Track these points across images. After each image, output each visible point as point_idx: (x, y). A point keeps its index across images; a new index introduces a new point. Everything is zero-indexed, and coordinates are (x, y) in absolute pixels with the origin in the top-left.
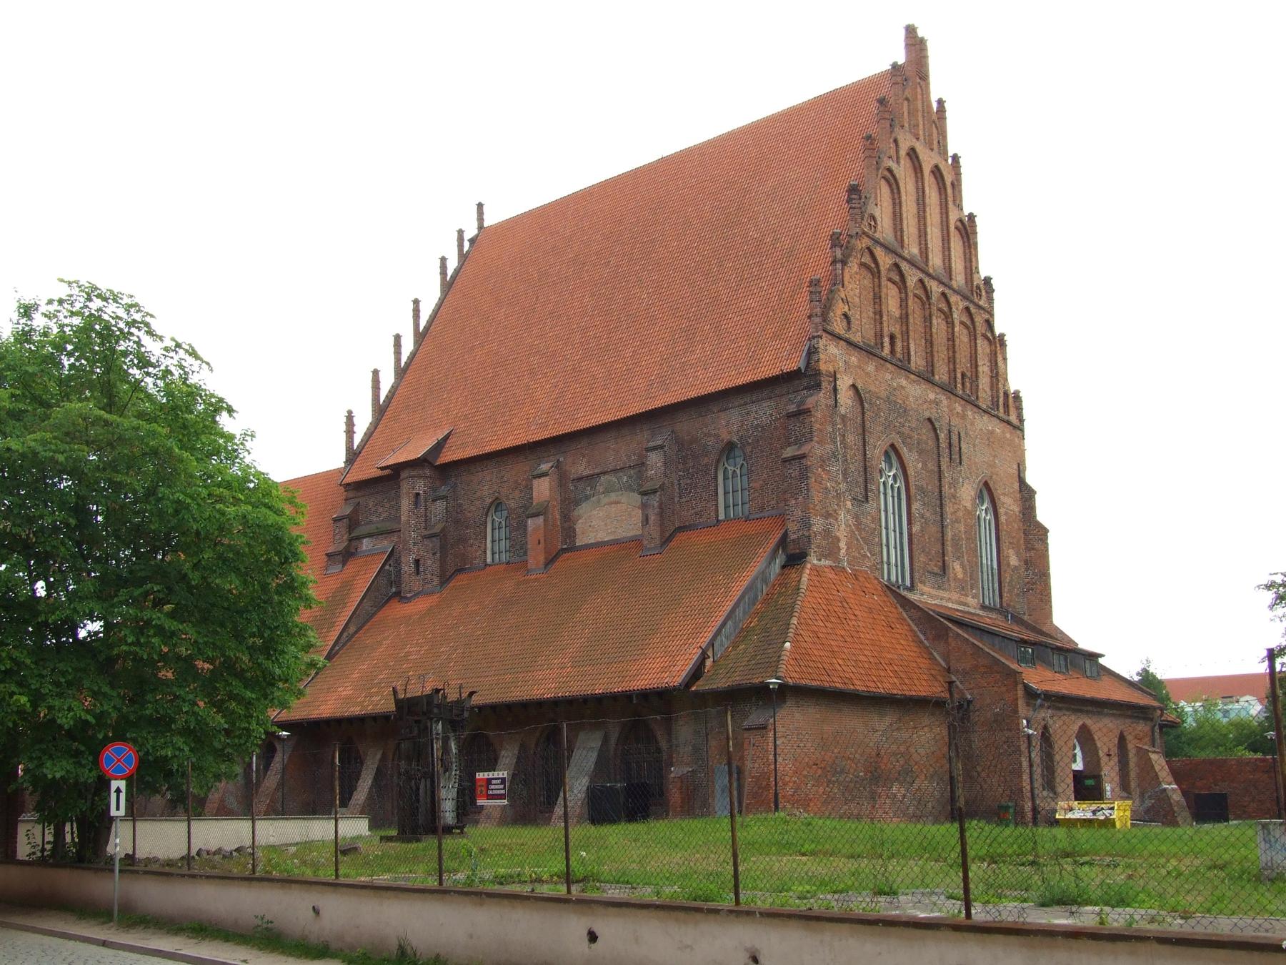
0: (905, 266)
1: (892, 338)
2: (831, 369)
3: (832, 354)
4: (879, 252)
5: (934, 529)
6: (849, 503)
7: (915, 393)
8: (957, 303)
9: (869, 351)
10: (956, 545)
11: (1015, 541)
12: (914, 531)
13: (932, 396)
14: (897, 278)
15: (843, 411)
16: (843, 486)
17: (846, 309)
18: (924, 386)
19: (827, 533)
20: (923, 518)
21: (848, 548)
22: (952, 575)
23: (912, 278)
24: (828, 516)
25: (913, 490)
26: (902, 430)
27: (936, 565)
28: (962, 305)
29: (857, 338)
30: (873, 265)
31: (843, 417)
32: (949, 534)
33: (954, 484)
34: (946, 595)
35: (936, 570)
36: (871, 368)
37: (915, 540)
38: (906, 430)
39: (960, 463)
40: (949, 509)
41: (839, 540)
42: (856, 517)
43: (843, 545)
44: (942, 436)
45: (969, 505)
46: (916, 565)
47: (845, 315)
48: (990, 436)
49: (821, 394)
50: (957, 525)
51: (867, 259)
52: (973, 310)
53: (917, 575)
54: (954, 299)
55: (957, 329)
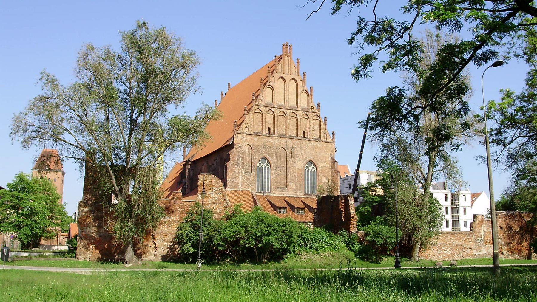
0: (273, 109)
1: (269, 129)
2: (239, 142)
3: (238, 138)
4: (262, 109)
5: (283, 176)
6: (243, 174)
7: (274, 142)
8: (300, 114)
9: (256, 134)
10: (293, 179)
11: (326, 175)
12: (272, 178)
13: (285, 141)
14: (272, 113)
15: (243, 152)
16: (241, 170)
17: (247, 126)
18: (280, 139)
19: (233, 182)
20: (277, 174)
21: (242, 185)
22: (289, 187)
23: (277, 112)
24: (234, 178)
25: (272, 167)
26: (268, 152)
27: (283, 186)
28: (302, 113)
29: (252, 132)
30: (260, 112)
31: (243, 153)
32: (289, 177)
33: (293, 163)
34: (286, 193)
35: (283, 187)
36: (256, 138)
37: (272, 180)
38: (271, 152)
39: (297, 157)
40: (290, 170)
41: (238, 183)
42: (246, 177)
43: (240, 185)
44: (288, 151)
45: (300, 168)
46: (272, 187)
47: (247, 127)
48: (314, 148)
49: (234, 149)
50: (293, 174)
51: (258, 111)
52: (307, 113)
53: (272, 189)
54: (297, 113)
55: (299, 121)
